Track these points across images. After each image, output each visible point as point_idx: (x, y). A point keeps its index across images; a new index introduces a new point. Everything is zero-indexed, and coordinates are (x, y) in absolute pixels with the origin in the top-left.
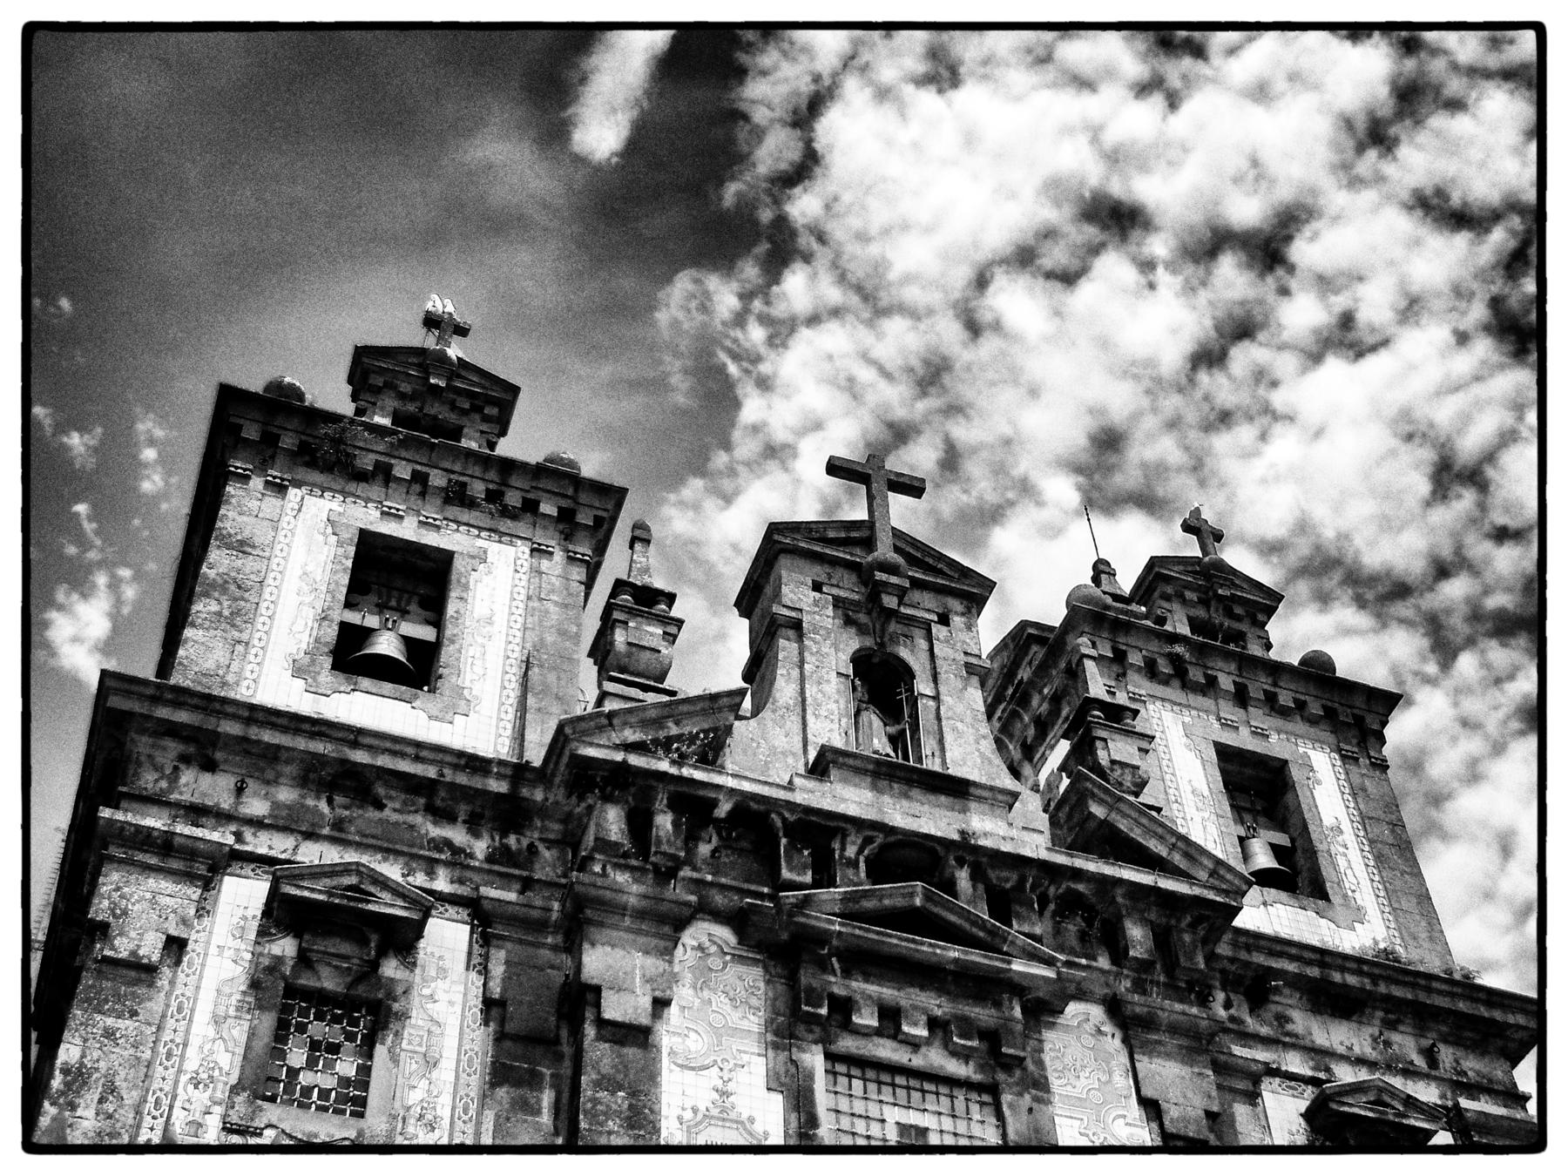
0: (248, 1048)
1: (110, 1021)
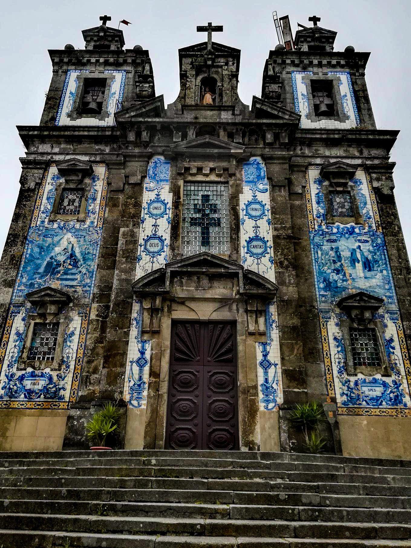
0: (54, 203)
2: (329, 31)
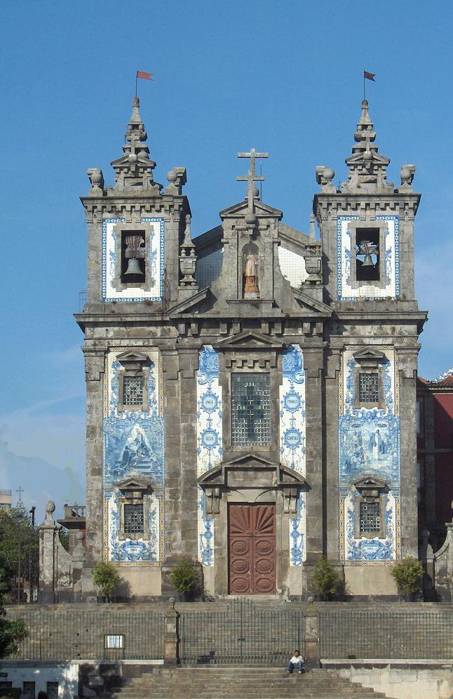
1: (93, 393)
2: (383, 157)
